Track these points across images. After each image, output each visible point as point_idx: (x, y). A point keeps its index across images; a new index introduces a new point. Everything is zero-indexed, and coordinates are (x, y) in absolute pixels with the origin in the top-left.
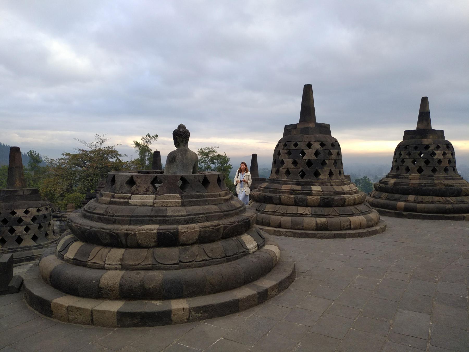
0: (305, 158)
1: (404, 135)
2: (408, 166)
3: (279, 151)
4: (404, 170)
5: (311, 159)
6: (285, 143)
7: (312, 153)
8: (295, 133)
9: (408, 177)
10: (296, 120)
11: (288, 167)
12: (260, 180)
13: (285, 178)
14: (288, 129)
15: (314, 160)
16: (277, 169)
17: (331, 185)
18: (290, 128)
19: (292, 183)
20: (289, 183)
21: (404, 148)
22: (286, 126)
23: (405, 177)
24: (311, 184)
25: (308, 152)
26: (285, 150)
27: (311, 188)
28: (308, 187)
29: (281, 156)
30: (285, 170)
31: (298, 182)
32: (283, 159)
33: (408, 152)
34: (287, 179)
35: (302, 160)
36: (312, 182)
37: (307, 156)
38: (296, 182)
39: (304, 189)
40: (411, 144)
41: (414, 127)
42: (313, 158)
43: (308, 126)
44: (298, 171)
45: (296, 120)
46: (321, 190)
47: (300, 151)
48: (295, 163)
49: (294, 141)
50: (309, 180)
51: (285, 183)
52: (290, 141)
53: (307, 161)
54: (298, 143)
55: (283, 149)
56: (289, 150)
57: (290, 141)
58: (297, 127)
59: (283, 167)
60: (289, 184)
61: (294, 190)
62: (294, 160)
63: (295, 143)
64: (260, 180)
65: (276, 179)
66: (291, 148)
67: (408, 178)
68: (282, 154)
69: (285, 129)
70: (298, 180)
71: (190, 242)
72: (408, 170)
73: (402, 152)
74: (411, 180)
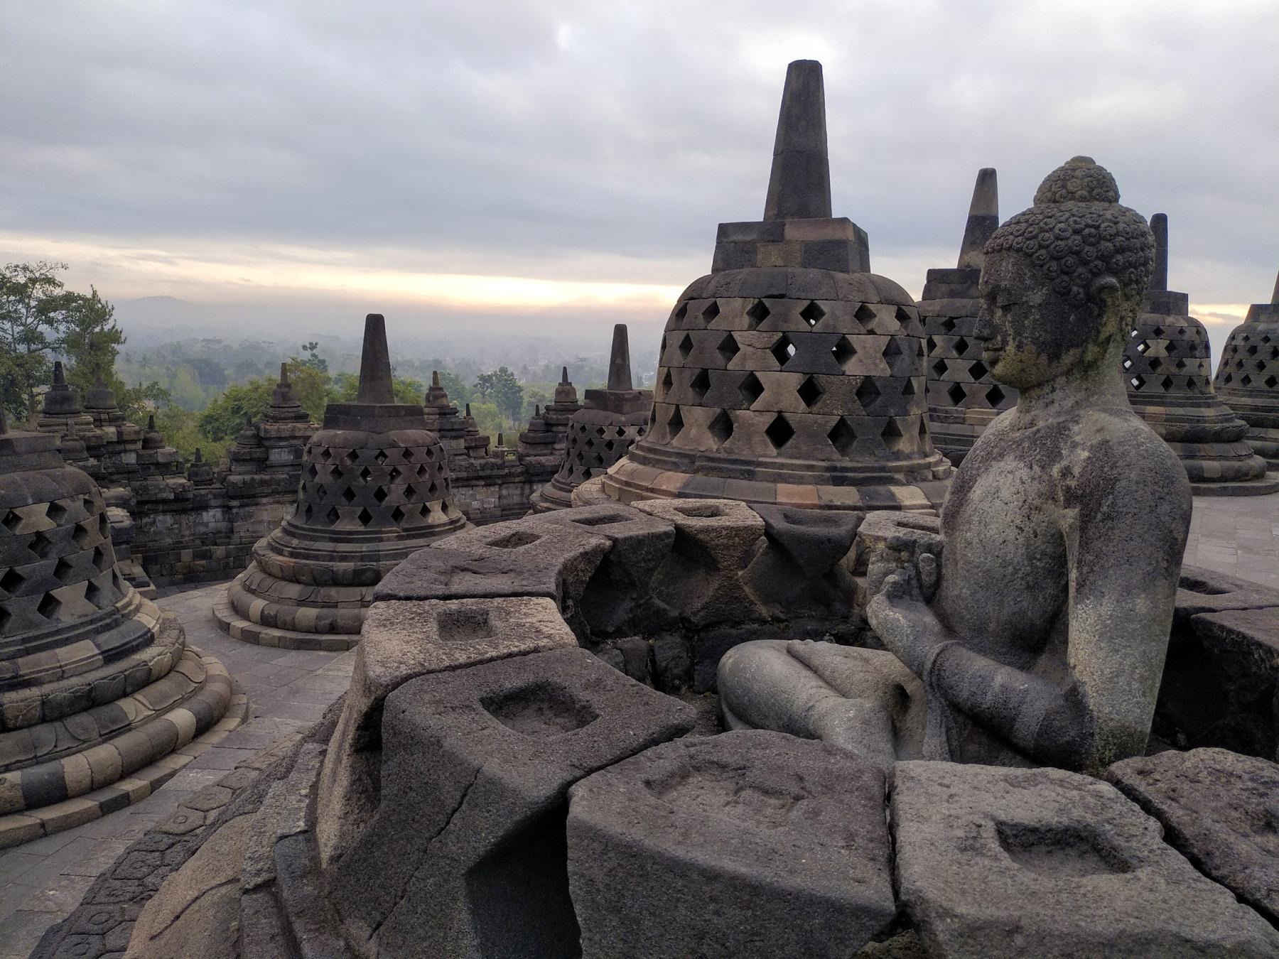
0: (853, 367)
1: (926, 282)
2: (959, 383)
3: (726, 334)
4: (947, 394)
5: (873, 374)
6: (756, 301)
7: (876, 352)
8: (773, 259)
9: (964, 418)
10: (752, 207)
11: (781, 406)
12: (406, 415)
13: (770, 453)
14: (736, 243)
15: (885, 378)
16: (718, 410)
17: (935, 477)
18: (748, 238)
19: (814, 477)
20: (802, 477)
21: (942, 324)
22: (724, 230)
23: (957, 418)
24: (887, 478)
25: (865, 348)
26: (765, 334)
27: (893, 496)
28: (881, 489)
29: (744, 359)
30: (768, 419)
31: (834, 469)
32: (752, 374)
33: (957, 338)
34: (779, 455)
35: (841, 378)
36: (883, 469)
37: (861, 361)
38: (828, 469)
39: (871, 498)
40: (964, 313)
41: (950, 261)
42: (882, 370)
43: (844, 237)
44: (826, 422)
45: (752, 207)
46: (925, 502)
47: (835, 339)
48: (810, 392)
49: (803, 295)
50: (868, 461)
51: (780, 475)
52: (782, 296)
53: (859, 385)
54: (824, 305)
55: (751, 328)
56: (783, 332)
57: (782, 296)
58: (783, 234)
59: (755, 406)
60: (800, 481)
61: (837, 508)
62: (808, 376)
63: (807, 303)
64: (404, 413)
65: (718, 455)
66: (792, 327)
67: (963, 421)
68: (750, 349)
69: (724, 240)
70: (829, 460)
71: (163, 674)
72: (957, 394)
73: (936, 339)
74: (976, 427)
